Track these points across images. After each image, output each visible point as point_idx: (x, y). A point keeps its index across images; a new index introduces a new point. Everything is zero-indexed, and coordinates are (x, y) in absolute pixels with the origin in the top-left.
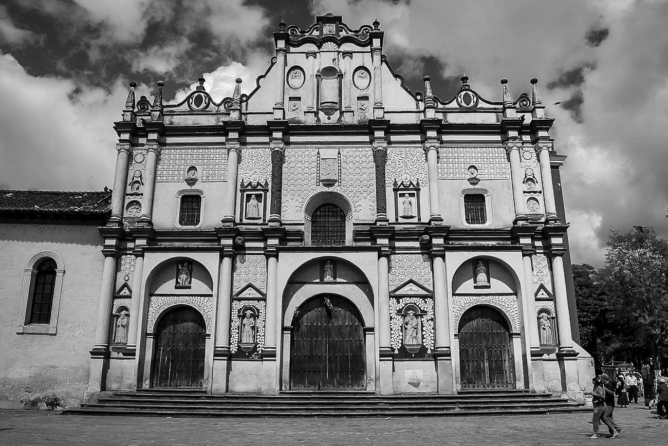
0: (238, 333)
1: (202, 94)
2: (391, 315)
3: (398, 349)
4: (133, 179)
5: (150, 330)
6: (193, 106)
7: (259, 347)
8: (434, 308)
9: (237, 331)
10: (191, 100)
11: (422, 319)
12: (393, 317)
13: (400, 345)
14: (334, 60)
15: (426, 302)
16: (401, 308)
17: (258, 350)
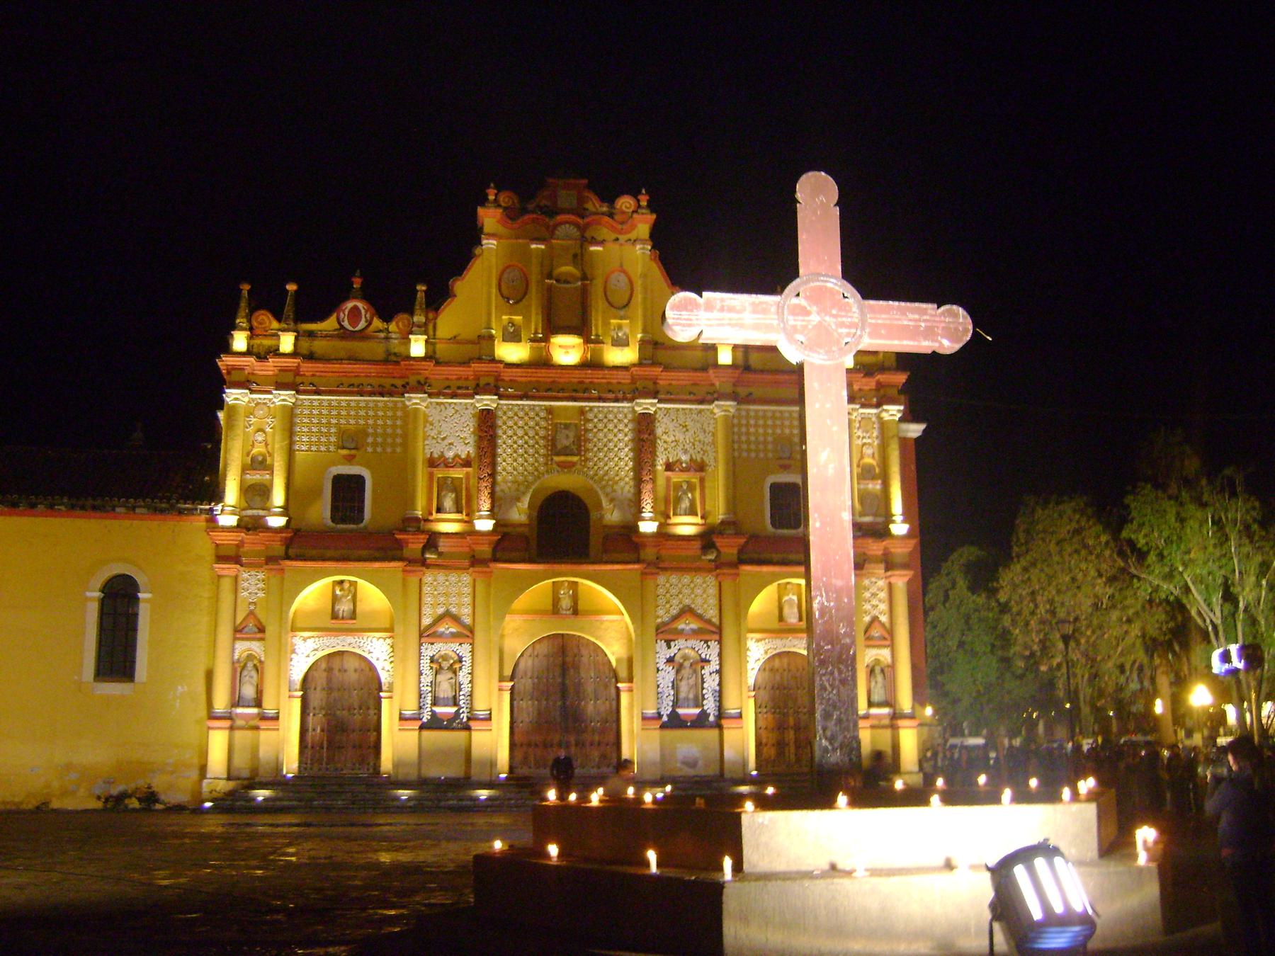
0: (431, 692)
1: (360, 305)
2: (658, 665)
3: (667, 715)
4: (253, 446)
5: (298, 686)
6: (346, 324)
7: (463, 712)
8: (720, 655)
9: (429, 689)
10: (342, 315)
11: (703, 672)
12: (660, 668)
13: (670, 709)
14: (575, 256)
15: (708, 647)
16: (672, 655)
17: (461, 716)
